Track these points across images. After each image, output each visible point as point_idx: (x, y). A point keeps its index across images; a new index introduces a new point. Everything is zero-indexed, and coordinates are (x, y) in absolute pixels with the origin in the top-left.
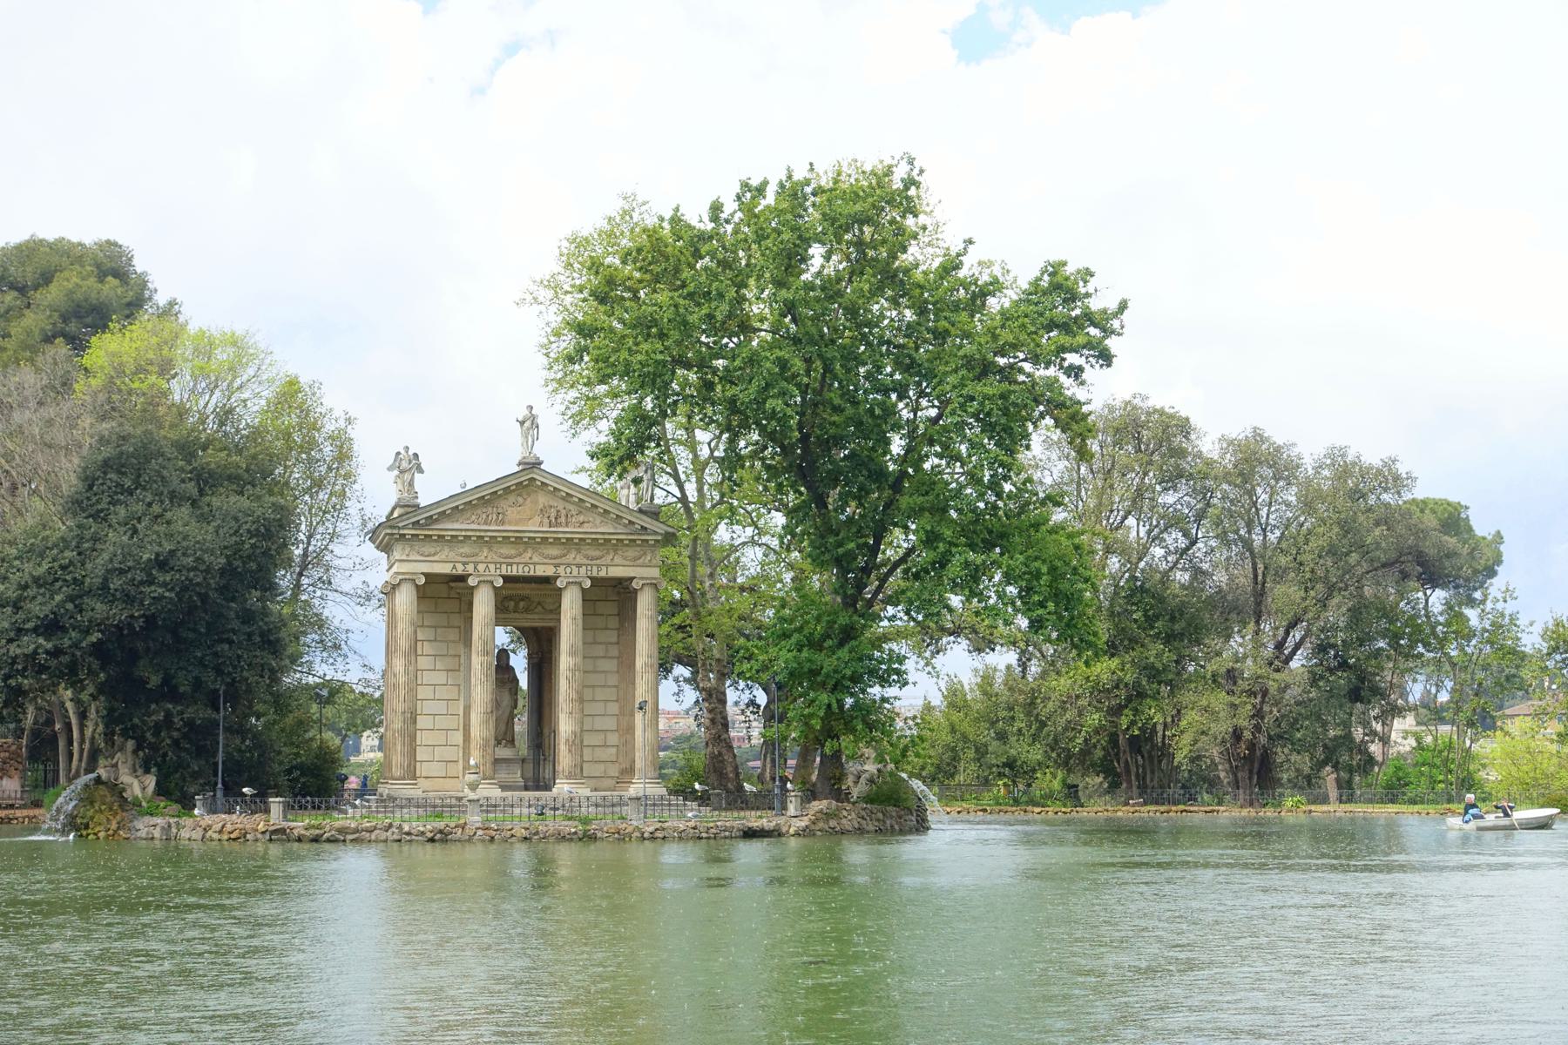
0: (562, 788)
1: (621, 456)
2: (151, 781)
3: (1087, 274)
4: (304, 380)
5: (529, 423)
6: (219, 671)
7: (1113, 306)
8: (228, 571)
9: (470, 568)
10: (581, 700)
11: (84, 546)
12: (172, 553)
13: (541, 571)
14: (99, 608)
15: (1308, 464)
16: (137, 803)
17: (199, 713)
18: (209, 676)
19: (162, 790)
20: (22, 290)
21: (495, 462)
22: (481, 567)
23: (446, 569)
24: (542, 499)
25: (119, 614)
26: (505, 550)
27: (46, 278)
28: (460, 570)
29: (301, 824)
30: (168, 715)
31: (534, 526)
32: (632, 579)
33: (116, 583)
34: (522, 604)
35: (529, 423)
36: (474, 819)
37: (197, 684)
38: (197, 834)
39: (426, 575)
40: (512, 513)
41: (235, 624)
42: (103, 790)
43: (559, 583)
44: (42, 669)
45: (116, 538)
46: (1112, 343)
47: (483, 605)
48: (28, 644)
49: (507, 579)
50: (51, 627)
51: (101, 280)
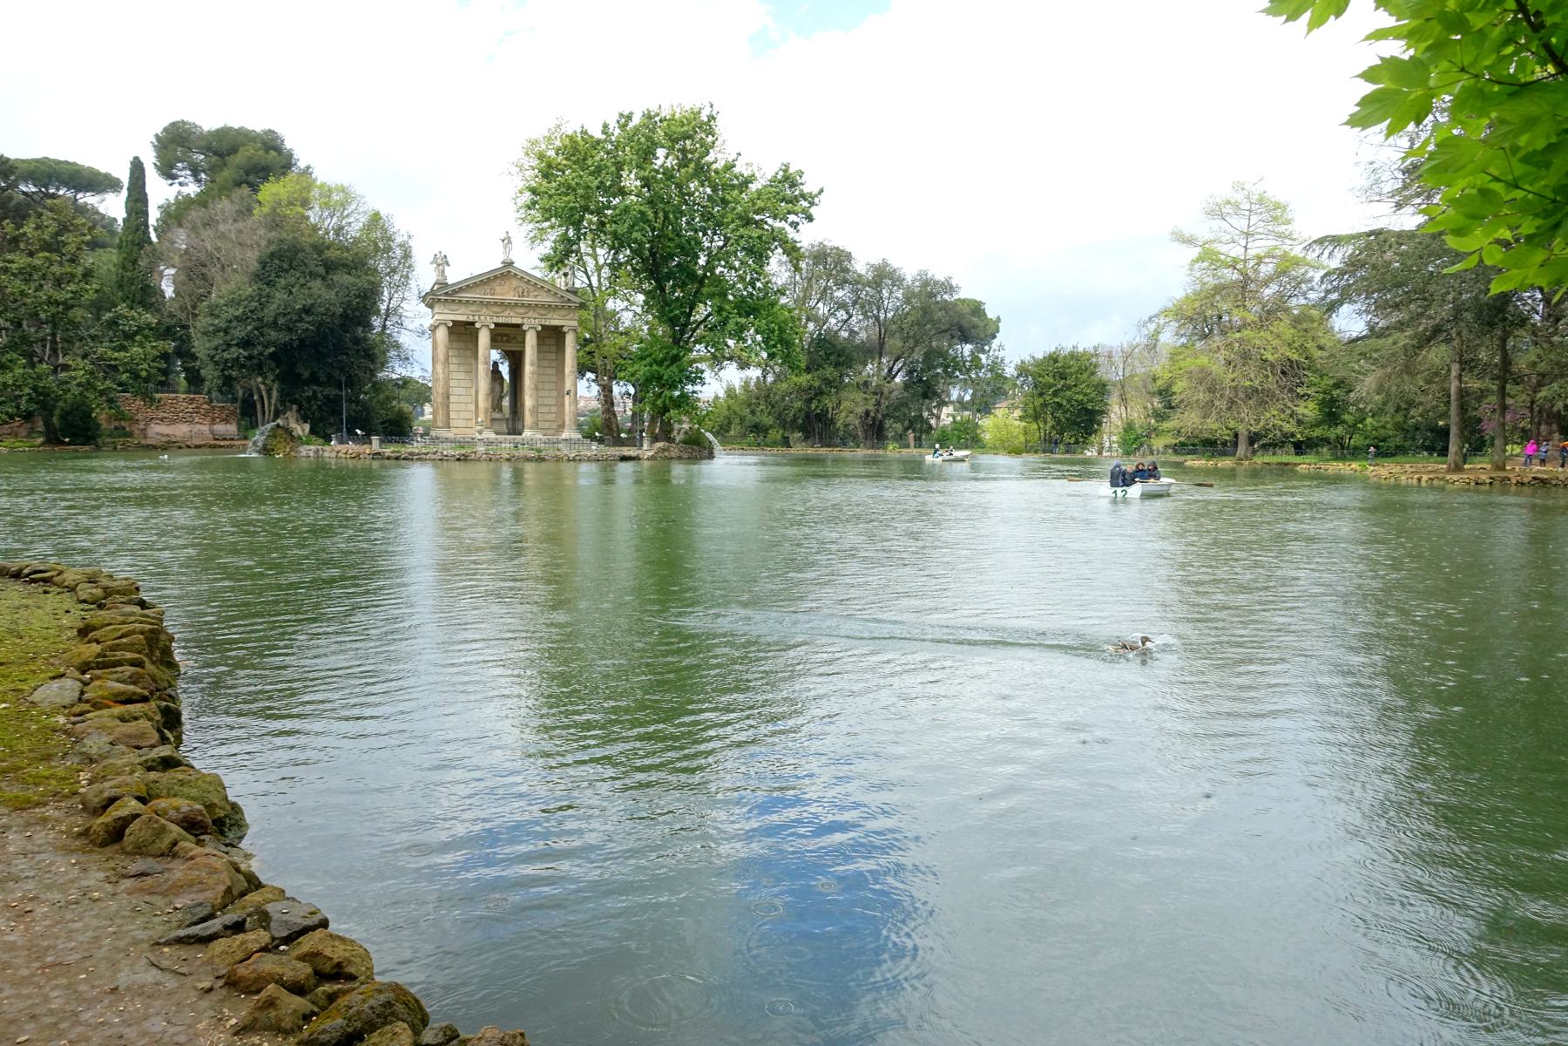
0: (527, 434)
1: (557, 261)
2: (307, 427)
3: (801, 173)
4: (383, 213)
5: (507, 241)
6: (342, 370)
7: (815, 192)
8: (344, 316)
10: (537, 389)
11: (263, 300)
13: (515, 321)
14: (273, 335)
15: (909, 279)
16: (300, 438)
17: (331, 392)
18: (336, 373)
19: (312, 431)
21: (491, 262)
23: (463, 318)
24: (515, 283)
25: (284, 337)
26: (495, 309)
27: (234, 150)
28: (471, 319)
29: (388, 450)
30: (315, 392)
31: (511, 297)
33: (281, 321)
35: (507, 241)
36: (481, 449)
37: (330, 377)
38: (333, 455)
40: (498, 289)
41: (350, 345)
42: (280, 431)
44: (243, 366)
45: (280, 296)
46: (813, 210)
47: (484, 338)
48: (235, 352)
49: (497, 325)
50: (246, 343)
51: (267, 152)
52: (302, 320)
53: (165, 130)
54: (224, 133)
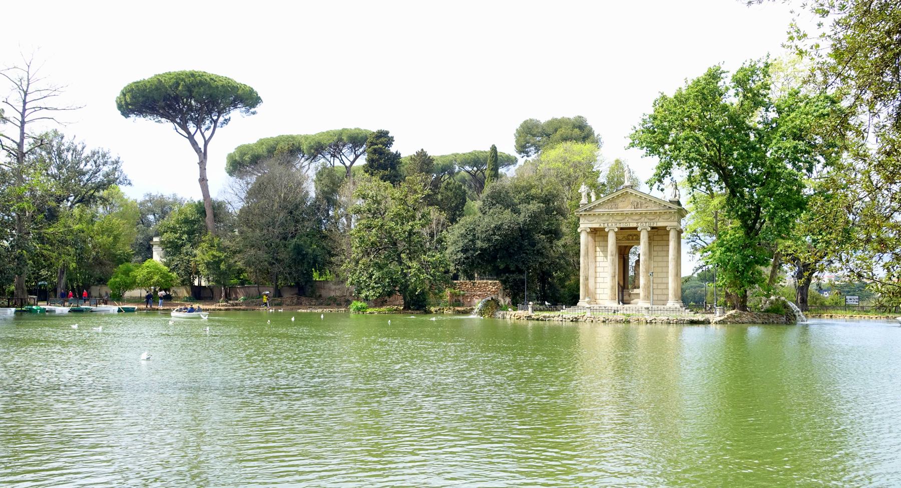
12: (502, 224)
13: (632, 225)
14: (479, 244)
18: (520, 265)
20: (548, 135)
23: (597, 226)
24: (632, 199)
25: (485, 245)
27: (556, 130)
28: (602, 226)
29: (535, 315)
30: (508, 278)
31: (629, 209)
37: (517, 267)
40: (620, 205)
42: (493, 302)
44: (464, 263)
52: (494, 234)
53: (521, 126)
54: (550, 123)
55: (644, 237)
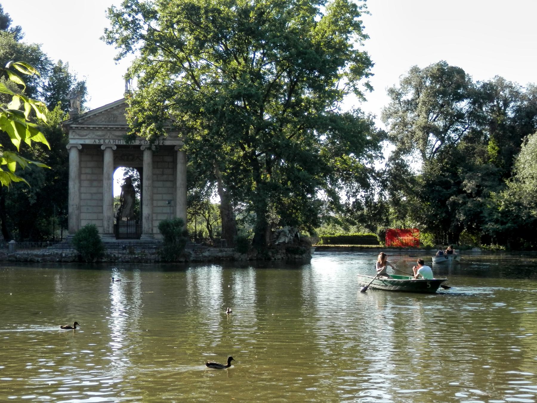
9: (102, 142)
22: (107, 141)
28: (97, 142)
32: (175, 146)
34: (130, 157)
39: (82, 144)
43: (141, 148)
55: (147, 157)
